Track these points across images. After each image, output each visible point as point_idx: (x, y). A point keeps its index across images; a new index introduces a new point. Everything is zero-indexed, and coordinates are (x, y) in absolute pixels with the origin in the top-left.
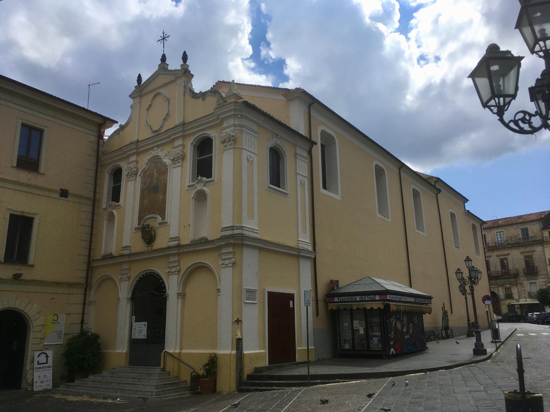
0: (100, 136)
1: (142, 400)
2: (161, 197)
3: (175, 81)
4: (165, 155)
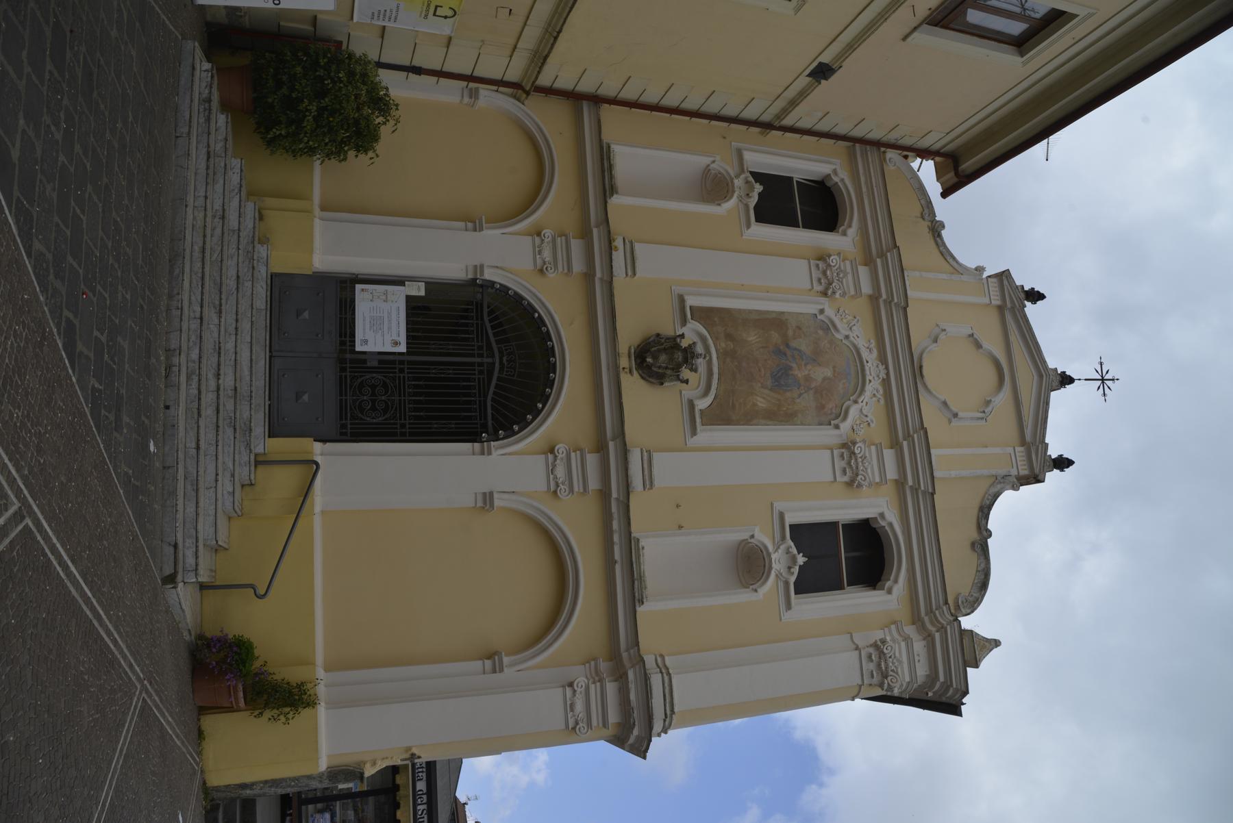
0: (924, 154)
1: (168, 571)
2: (762, 403)
3: (1023, 442)
4: (865, 413)
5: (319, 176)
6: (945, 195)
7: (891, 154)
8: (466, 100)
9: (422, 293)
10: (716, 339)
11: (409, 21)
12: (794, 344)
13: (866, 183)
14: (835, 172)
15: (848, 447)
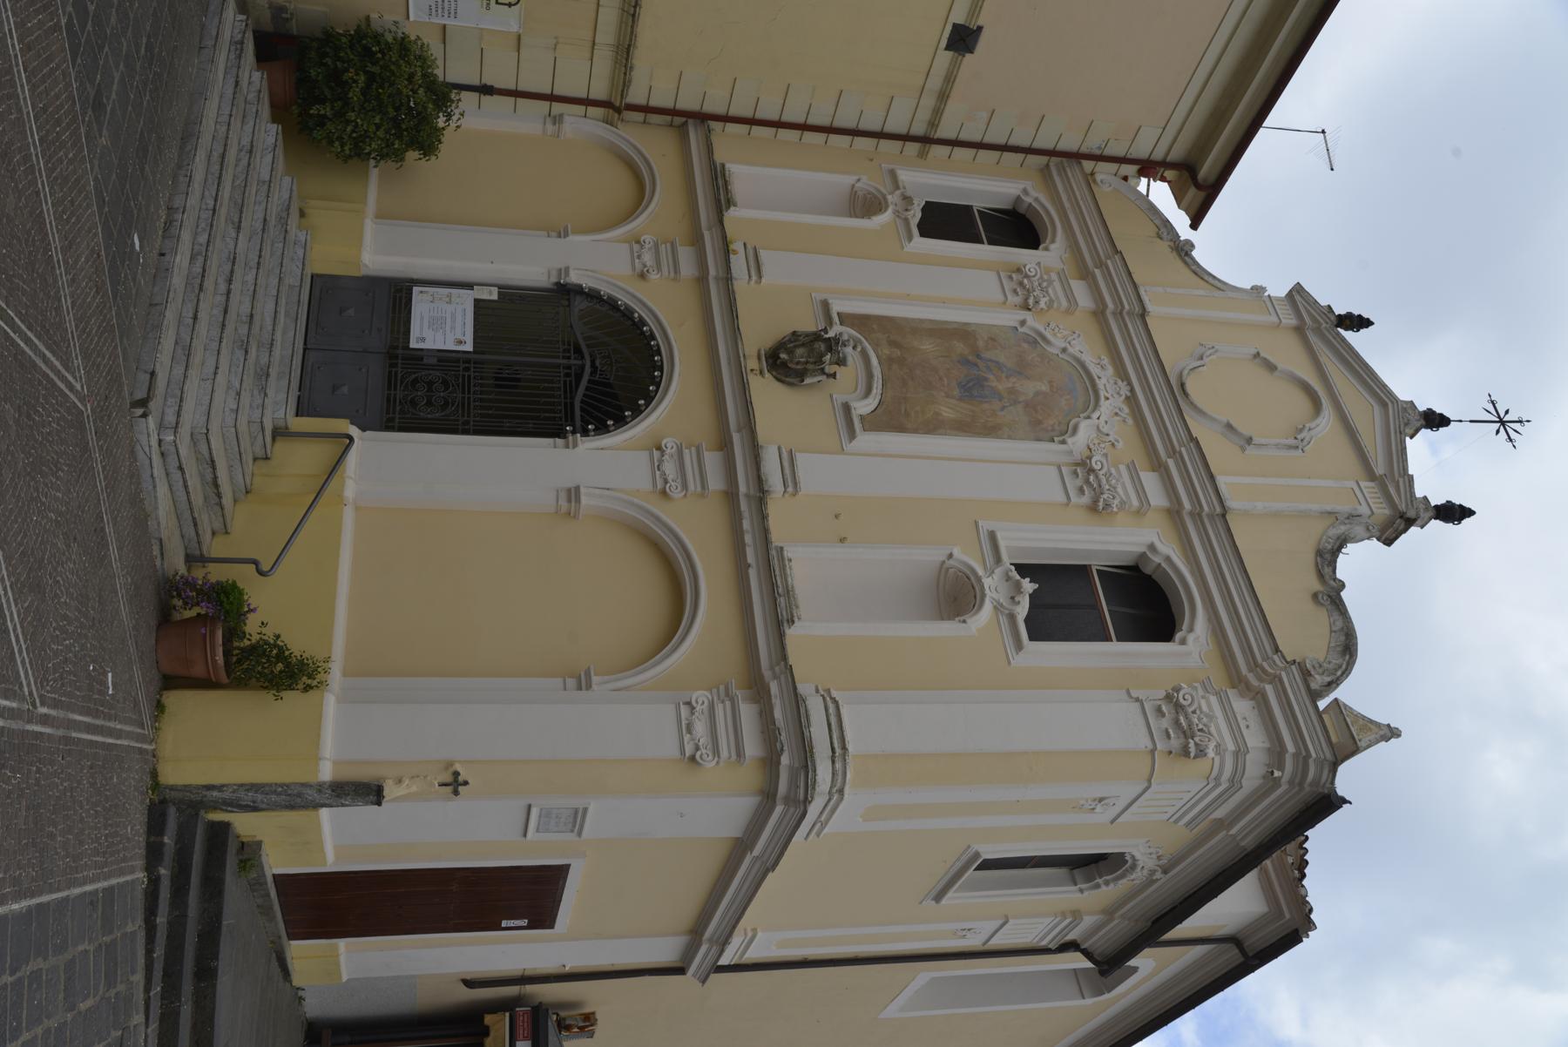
0: (1149, 168)
1: (140, 394)
2: (947, 413)
3: (1371, 476)
4: (1104, 427)
5: (374, 183)
6: (1195, 225)
7: (1104, 171)
8: (550, 128)
9: (495, 297)
10: (876, 346)
11: (470, 15)
12: (987, 355)
13: (1069, 199)
14: (1025, 191)
15: (1084, 466)
